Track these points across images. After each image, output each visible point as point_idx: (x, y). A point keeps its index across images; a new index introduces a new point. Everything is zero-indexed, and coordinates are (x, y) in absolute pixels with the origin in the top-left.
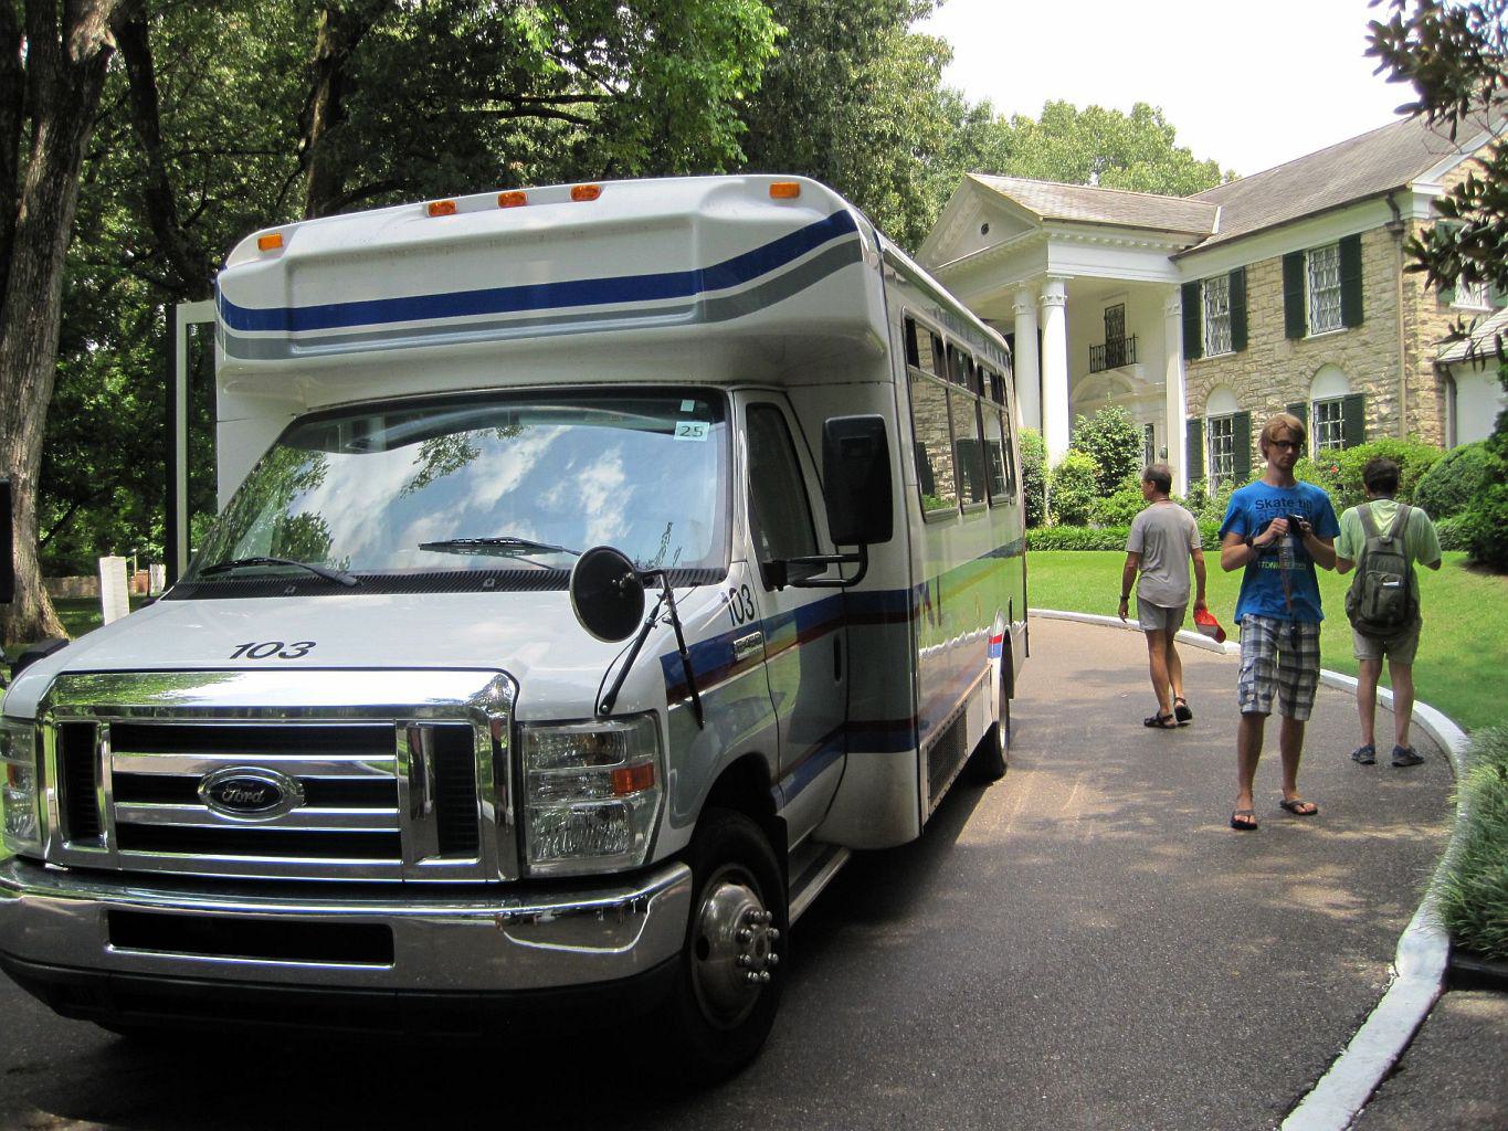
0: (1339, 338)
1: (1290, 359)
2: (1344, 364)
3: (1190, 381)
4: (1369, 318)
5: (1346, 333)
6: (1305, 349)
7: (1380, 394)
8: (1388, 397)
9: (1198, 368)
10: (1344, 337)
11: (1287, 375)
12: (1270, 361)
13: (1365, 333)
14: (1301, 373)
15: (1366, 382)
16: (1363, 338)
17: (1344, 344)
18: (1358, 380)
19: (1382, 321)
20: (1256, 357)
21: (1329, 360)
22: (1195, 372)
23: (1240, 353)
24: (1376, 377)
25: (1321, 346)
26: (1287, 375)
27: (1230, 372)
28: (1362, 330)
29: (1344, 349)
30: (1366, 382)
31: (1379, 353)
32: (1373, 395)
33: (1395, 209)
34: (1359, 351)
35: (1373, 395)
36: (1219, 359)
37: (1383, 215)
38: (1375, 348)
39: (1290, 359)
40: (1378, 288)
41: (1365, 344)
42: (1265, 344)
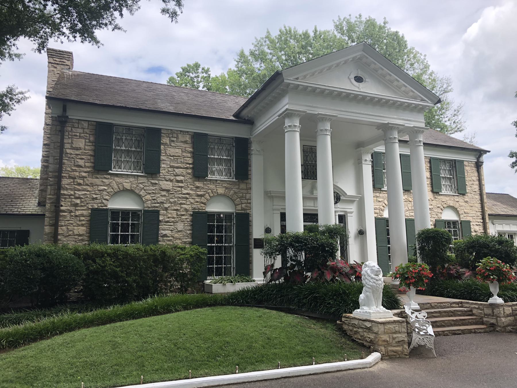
3: (375, 198)
6: (439, 197)
8: (478, 224)
13: (466, 198)
14: (438, 207)
18: (465, 215)
19: (473, 195)
21: (451, 205)
22: (378, 194)
25: (447, 198)
28: (465, 197)
33: (478, 159)
34: (464, 204)
37: (473, 159)
38: (470, 204)
40: (471, 183)
41: (466, 202)
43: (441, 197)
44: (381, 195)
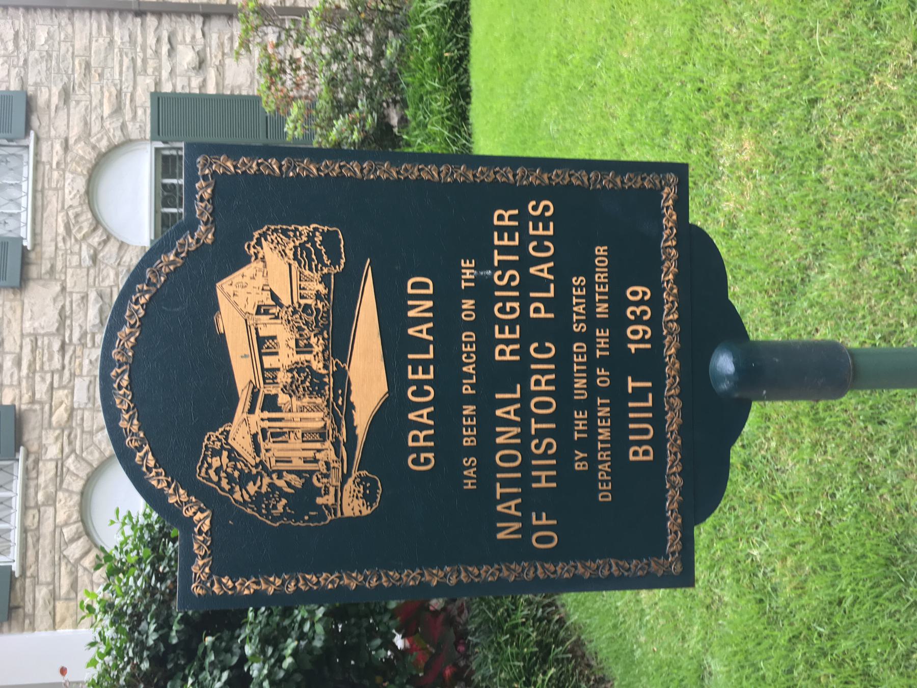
0: (44, 158)
1: (64, 289)
2: (94, 147)
3: (60, 605)
4: (23, 81)
5: (37, 139)
7: (158, 69)
9: (35, 577)
10: (45, 147)
11: (93, 295)
12: (56, 346)
13: (48, 95)
14: (94, 259)
15: (132, 95)
16: (55, 100)
17: (58, 147)
19: (34, 55)
20: (41, 390)
21: (81, 184)
23: (31, 435)
24: (128, 75)
25: (53, 204)
26: (93, 295)
27: (60, 464)
29: (66, 147)
30: (132, 95)
31: (88, 66)
32: (157, 84)
34: (77, 113)
35: (157, 84)
36: (25, 508)
38: (77, 77)
39: (64, 289)
41: (66, 95)
42: (18, 363)
43: (47, 237)
44: (45, 575)
